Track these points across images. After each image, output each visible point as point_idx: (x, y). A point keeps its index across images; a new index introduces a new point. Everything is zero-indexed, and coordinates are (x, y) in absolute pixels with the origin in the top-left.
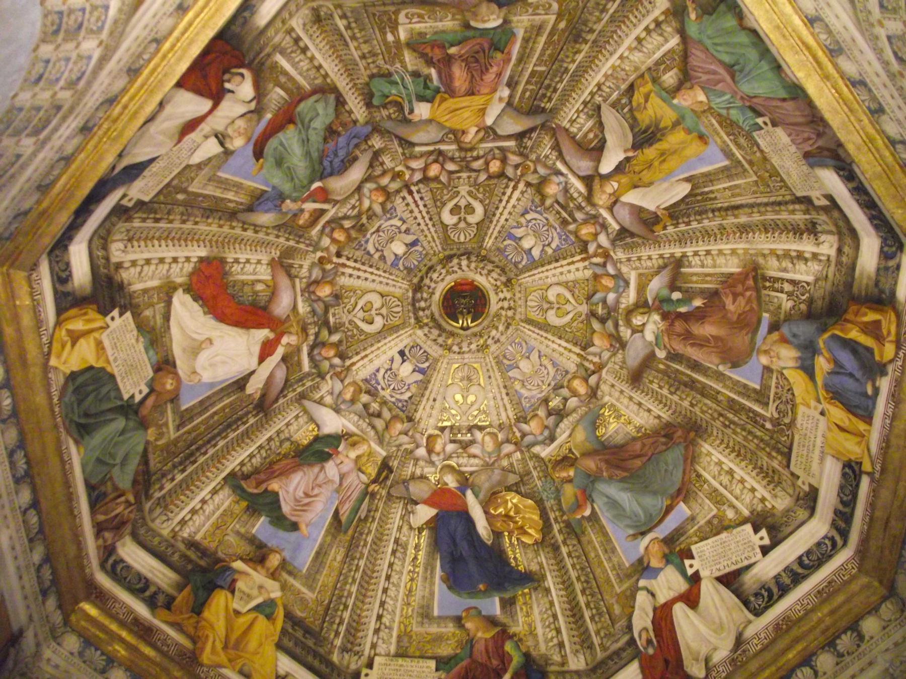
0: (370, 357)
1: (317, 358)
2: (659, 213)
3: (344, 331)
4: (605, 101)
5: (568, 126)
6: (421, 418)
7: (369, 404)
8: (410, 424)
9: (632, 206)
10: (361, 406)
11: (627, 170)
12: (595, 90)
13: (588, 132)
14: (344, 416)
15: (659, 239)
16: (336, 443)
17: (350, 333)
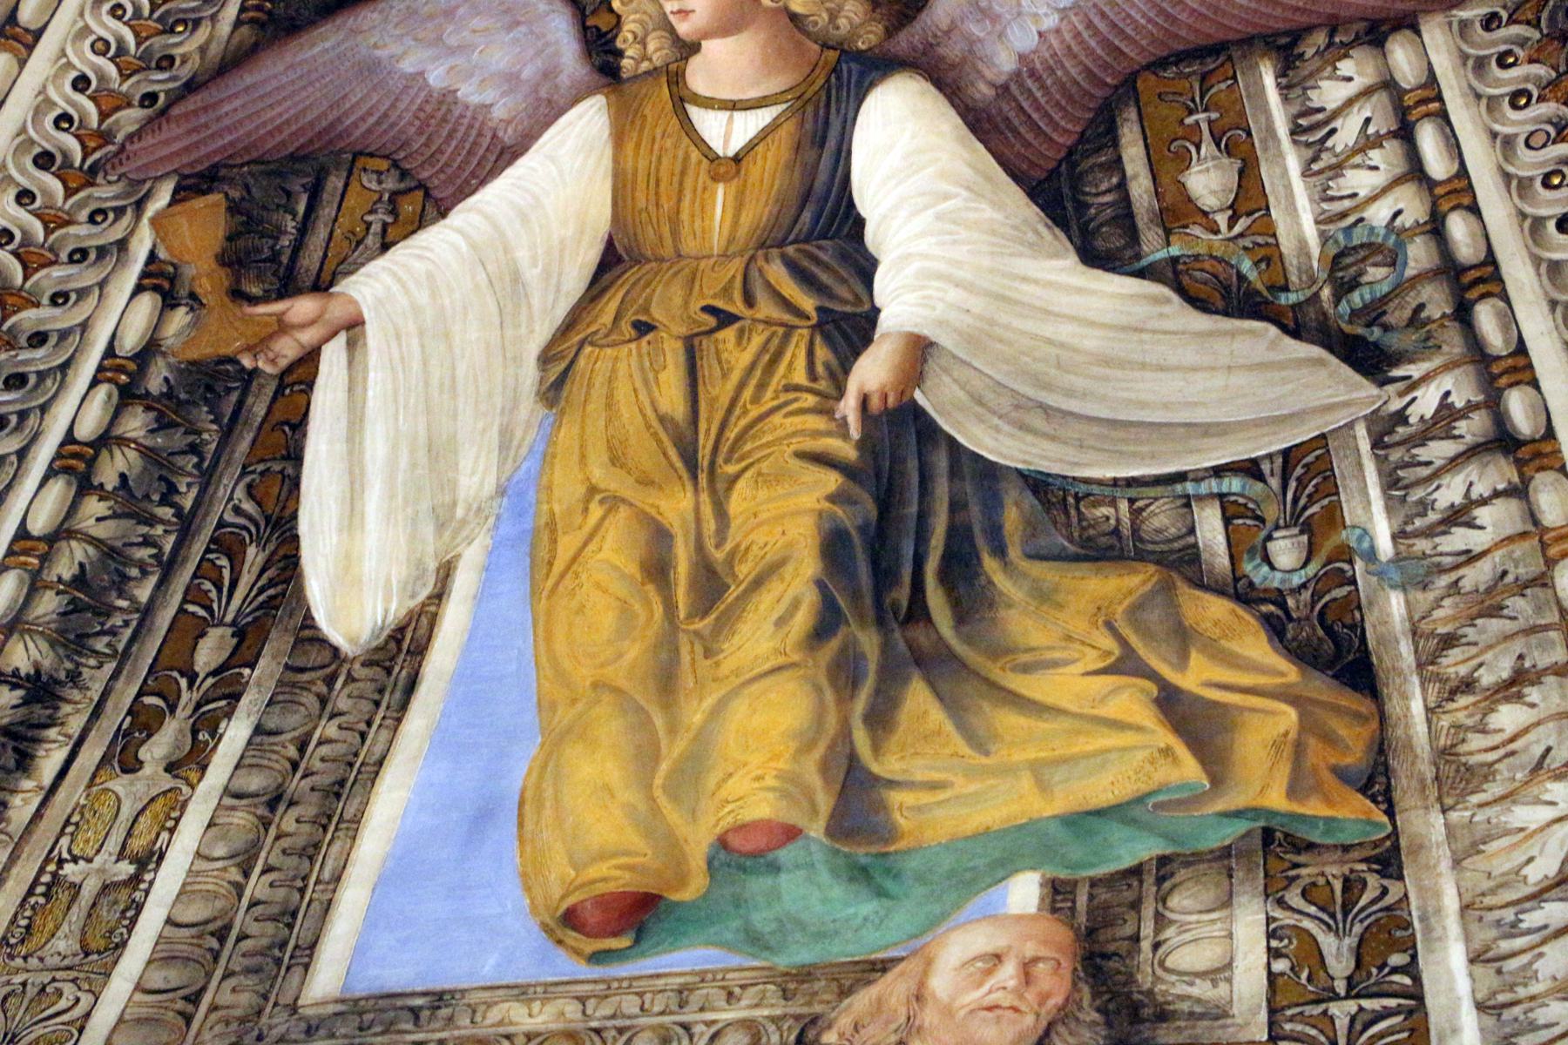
2: (302, 307)
4: (1385, 428)
5: (1402, 57)
9: (508, 154)
11: (777, 273)
12: (1517, 405)
13: (1248, 173)
15: (105, 192)
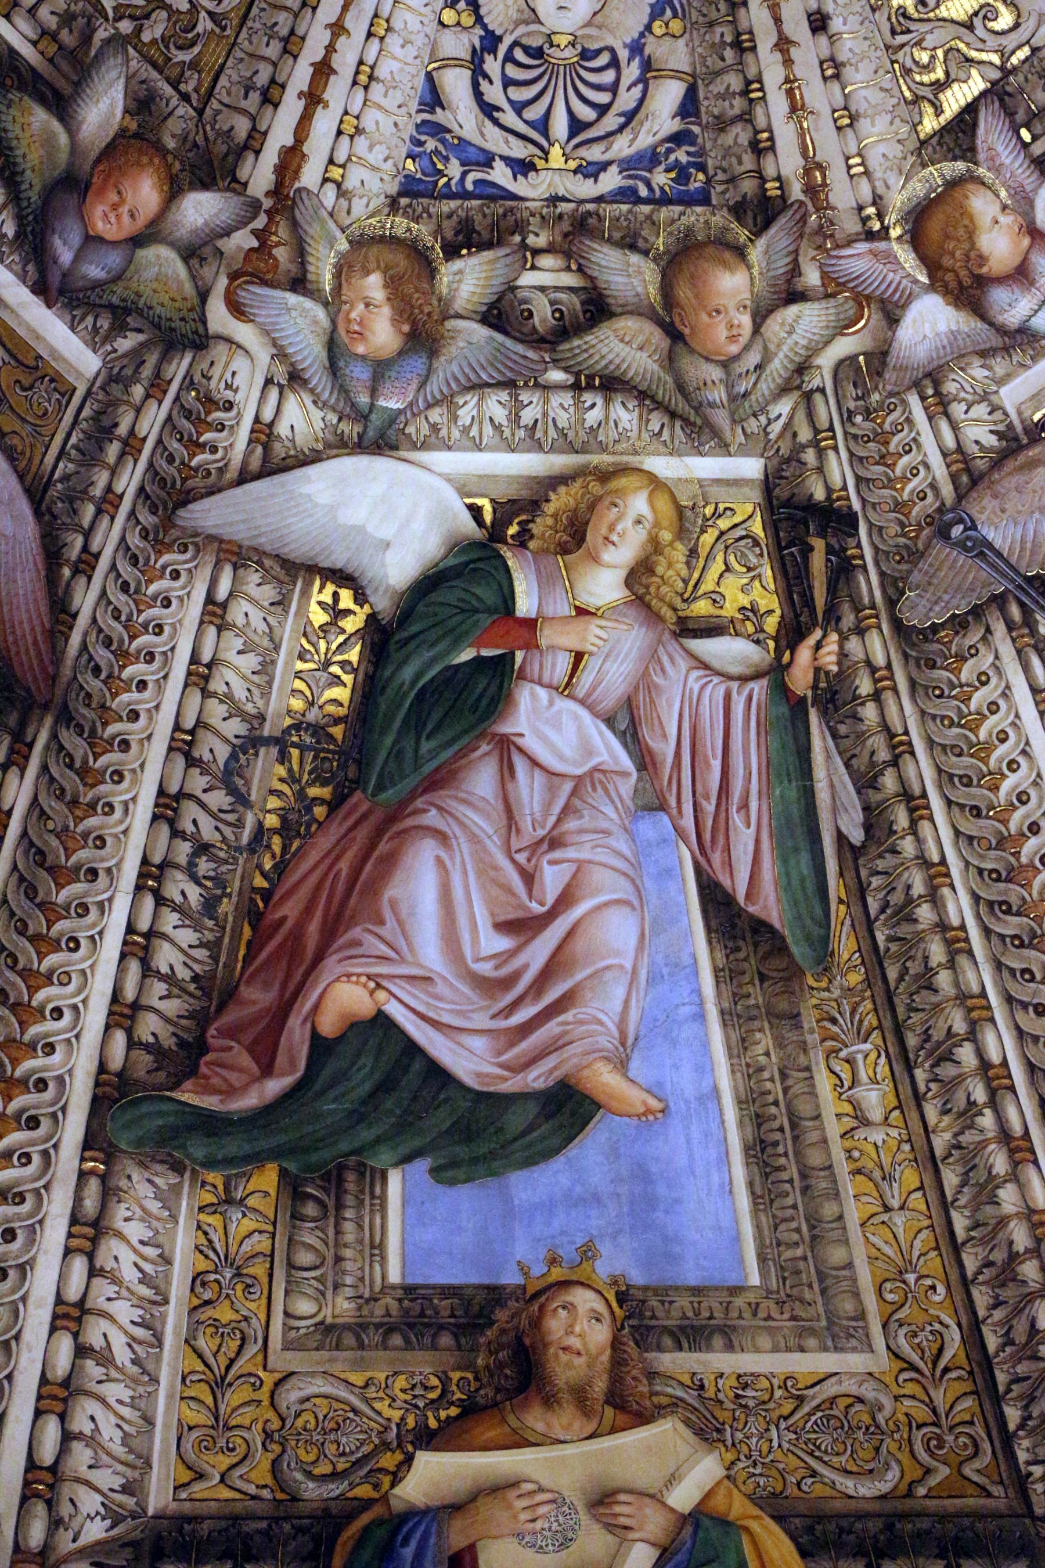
0: (345, 60)
1: (94, 271)
3: (115, 41)
6: (812, 166)
7: (512, 288)
8: (778, 235)
10: (481, 332)
14: (435, 441)
16: (487, 594)
17: (155, 29)
